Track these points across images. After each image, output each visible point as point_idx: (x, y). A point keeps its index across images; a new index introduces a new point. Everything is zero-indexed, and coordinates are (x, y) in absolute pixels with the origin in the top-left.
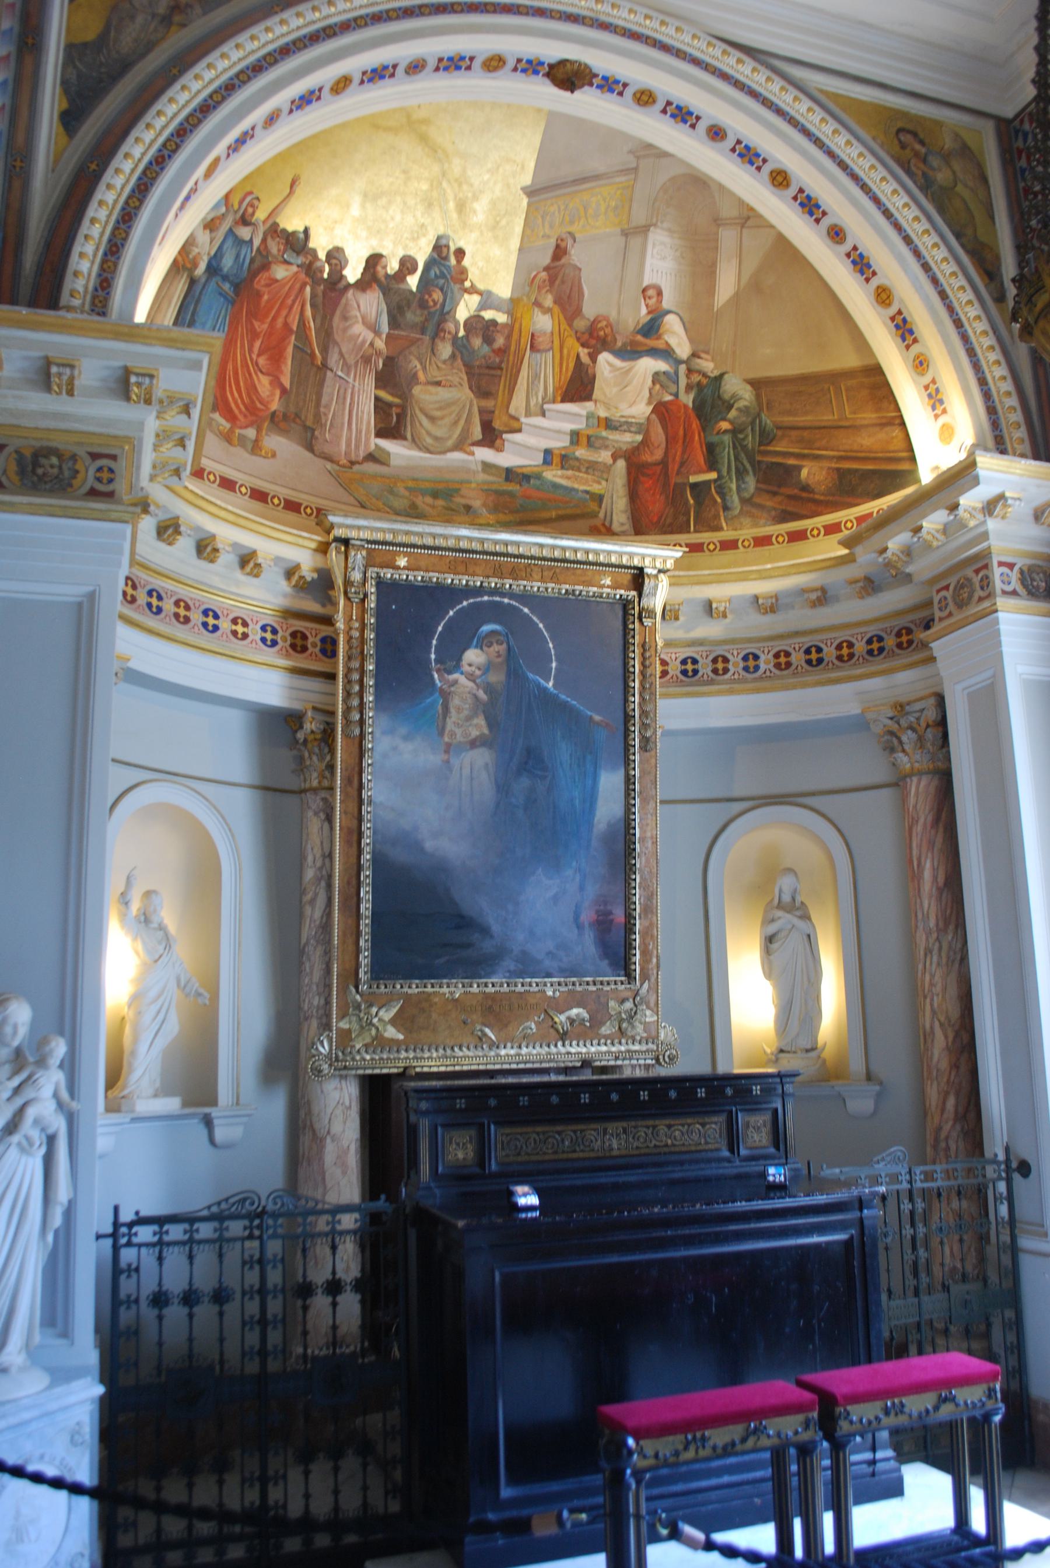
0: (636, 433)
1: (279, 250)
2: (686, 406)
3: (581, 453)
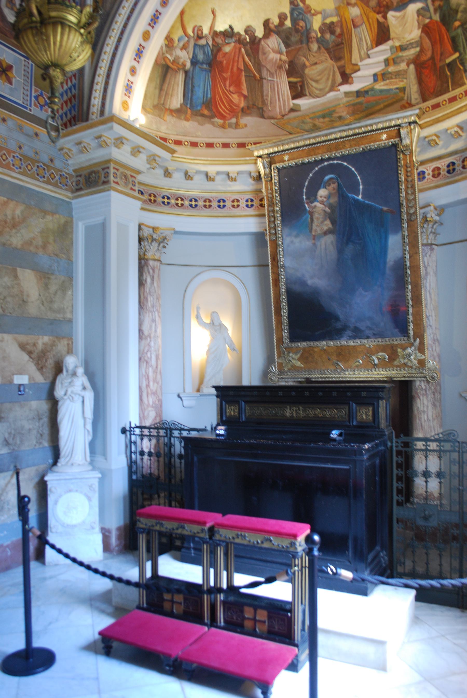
0: (416, 47)
1: (222, 41)
2: (437, 22)
3: (391, 69)
